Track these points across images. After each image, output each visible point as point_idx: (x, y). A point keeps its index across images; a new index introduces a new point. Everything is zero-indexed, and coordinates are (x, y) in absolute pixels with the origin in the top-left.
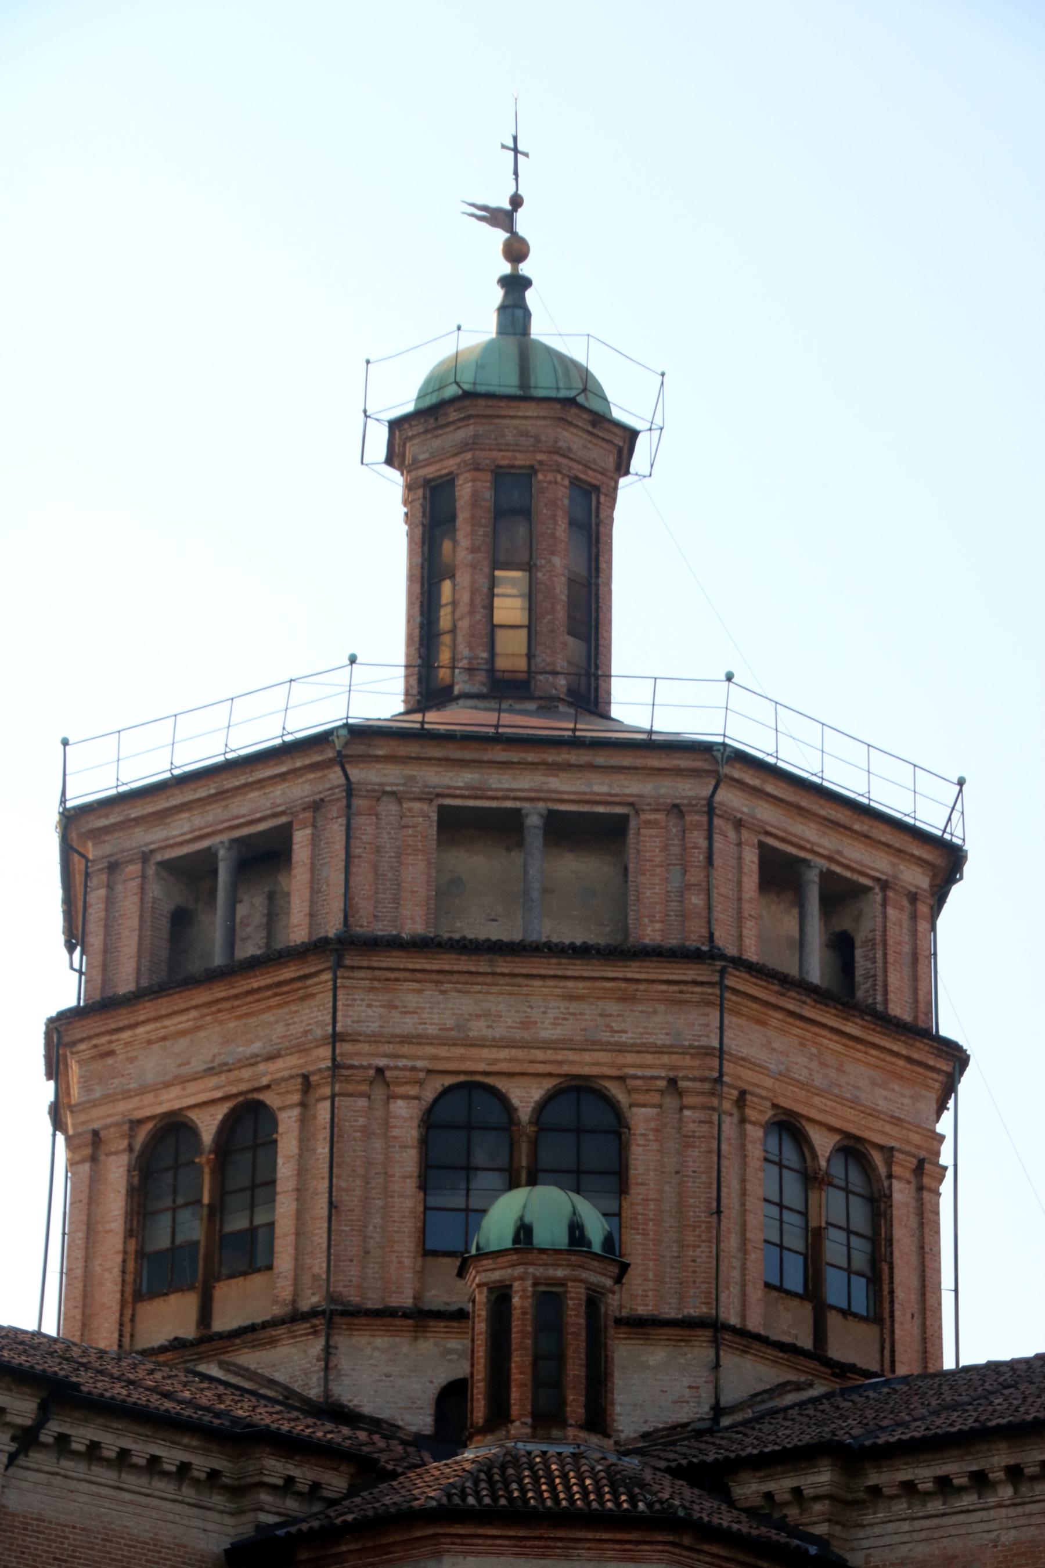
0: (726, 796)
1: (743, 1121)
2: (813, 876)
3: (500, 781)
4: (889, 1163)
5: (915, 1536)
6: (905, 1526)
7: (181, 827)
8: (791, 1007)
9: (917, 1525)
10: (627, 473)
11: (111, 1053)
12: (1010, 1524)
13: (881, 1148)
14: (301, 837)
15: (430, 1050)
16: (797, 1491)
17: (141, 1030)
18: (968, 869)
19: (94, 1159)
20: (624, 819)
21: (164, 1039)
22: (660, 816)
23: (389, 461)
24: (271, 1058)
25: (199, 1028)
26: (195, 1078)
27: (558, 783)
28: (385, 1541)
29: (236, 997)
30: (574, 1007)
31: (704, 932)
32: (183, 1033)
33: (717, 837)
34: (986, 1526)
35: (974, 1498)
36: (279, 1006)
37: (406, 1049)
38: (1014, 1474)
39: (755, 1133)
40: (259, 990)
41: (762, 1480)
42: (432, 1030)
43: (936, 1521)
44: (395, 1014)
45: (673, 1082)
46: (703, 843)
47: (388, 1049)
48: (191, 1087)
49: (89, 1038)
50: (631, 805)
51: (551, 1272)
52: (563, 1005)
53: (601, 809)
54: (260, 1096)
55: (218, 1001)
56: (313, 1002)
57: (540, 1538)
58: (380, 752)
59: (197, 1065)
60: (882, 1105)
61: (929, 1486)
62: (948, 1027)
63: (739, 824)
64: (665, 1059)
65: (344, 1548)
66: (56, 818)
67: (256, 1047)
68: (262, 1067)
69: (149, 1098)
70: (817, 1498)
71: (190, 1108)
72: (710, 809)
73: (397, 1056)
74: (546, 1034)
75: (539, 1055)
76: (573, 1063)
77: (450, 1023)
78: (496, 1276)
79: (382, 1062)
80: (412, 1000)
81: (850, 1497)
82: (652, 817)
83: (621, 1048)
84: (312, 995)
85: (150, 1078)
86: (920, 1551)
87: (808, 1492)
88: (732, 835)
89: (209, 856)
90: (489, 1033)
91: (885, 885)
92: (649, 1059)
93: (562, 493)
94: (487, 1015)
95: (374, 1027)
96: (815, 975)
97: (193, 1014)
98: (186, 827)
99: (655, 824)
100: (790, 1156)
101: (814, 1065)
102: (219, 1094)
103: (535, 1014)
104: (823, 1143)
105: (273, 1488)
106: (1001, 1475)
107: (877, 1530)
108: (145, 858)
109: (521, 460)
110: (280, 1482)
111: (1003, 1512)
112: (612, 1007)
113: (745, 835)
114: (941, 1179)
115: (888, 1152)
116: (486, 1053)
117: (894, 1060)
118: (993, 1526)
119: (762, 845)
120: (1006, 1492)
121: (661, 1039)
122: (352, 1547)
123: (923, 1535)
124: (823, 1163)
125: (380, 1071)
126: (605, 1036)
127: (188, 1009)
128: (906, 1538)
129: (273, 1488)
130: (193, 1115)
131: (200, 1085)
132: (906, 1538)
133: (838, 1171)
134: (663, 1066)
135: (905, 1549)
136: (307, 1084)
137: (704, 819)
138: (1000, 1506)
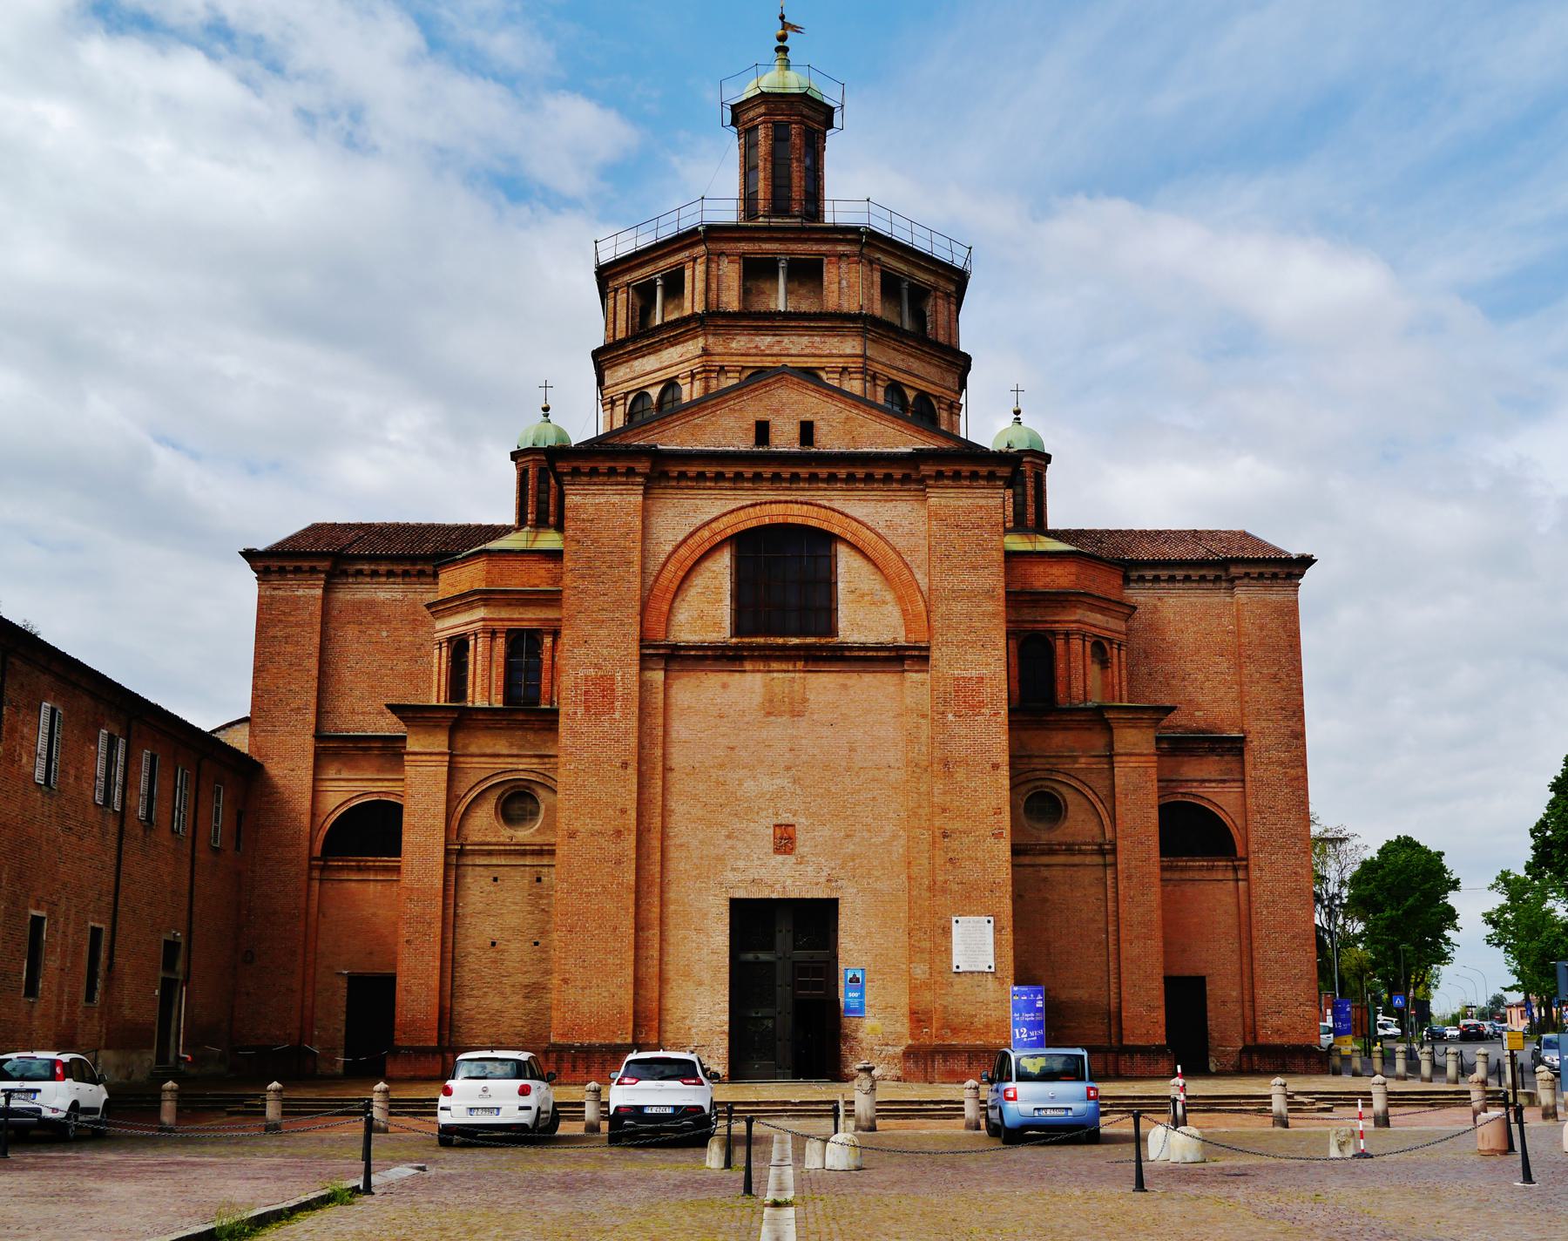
1: (875, 385)
10: (832, 127)
13: (935, 397)
14: (688, 273)
19: (612, 409)
23: (733, 124)
27: (794, 247)
62: (964, 347)
66: (594, 269)
91: (936, 289)
96: (907, 327)
100: (896, 399)
104: (911, 395)
108: (628, 285)
114: (960, 410)
119: (882, 272)
136: (693, 376)
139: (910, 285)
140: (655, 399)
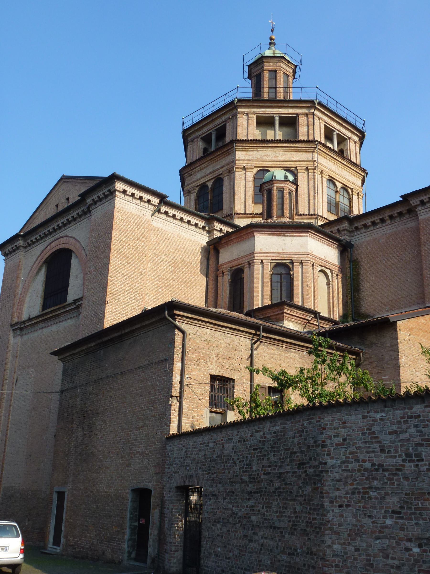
0: (316, 112)
2: (335, 133)
3: (269, 110)
4: (352, 191)
5: (366, 236)
6: (364, 234)
7: (205, 129)
8: (332, 155)
9: (367, 233)
11: (192, 175)
12: (390, 228)
15: (255, 162)
16: (338, 230)
17: (197, 168)
18: (366, 137)
20: (295, 118)
21: (201, 169)
22: (303, 116)
23: (248, 78)
24: (222, 168)
25: (208, 166)
26: (208, 175)
28: (241, 235)
29: (215, 157)
30: (286, 153)
31: (313, 138)
32: (205, 168)
33: (315, 120)
34: (383, 231)
35: (381, 225)
36: (223, 158)
37: (250, 162)
38: (391, 217)
39: (325, 180)
40: (220, 154)
41: (330, 228)
42: (255, 159)
43: (371, 232)
44: (248, 156)
45: (307, 168)
46: (312, 121)
47: (245, 162)
48: (206, 177)
49: (187, 172)
50: (297, 114)
51: (280, 185)
52: (283, 153)
53: (291, 115)
54: (220, 176)
55: (212, 159)
56: (230, 155)
57: (278, 231)
58: (244, 105)
59: (208, 173)
60: (350, 180)
61: (370, 224)
63: (320, 119)
64: (305, 163)
65: (232, 238)
67: (219, 167)
68: (220, 170)
69: (199, 181)
70: (343, 230)
71: (206, 182)
72: (314, 114)
73: (248, 164)
74: (279, 159)
75: (278, 163)
76: (285, 164)
77: (259, 157)
78: (268, 187)
79: (244, 165)
80: (251, 153)
81: (350, 230)
82: (301, 116)
83: (295, 161)
84: (230, 154)
85: (199, 177)
86: (367, 239)
87: (341, 229)
88: (318, 121)
89: (211, 134)
90: (267, 159)
91: (350, 138)
92: (302, 163)
93: (282, 74)
94: (267, 155)
95: (243, 158)
97: (207, 163)
98: (206, 129)
99: (302, 118)
101: (336, 169)
102: (212, 177)
103: (277, 155)
104: (339, 186)
105: (217, 230)
106: (388, 218)
107: (357, 237)
109: (274, 69)
110: (219, 229)
111: (388, 226)
112: (294, 153)
113: (321, 121)
115: (352, 189)
116: (267, 163)
117: (353, 171)
118: (385, 230)
120: (389, 222)
121: (304, 159)
122: (234, 238)
123: (368, 235)
124: (339, 189)
125: (244, 167)
126: (293, 159)
127: (206, 162)
128: (364, 237)
129: (217, 230)
130: (207, 183)
131: (208, 176)
132: (364, 237)
133: (342, 191)
134: (305, 164)
135: (363, 240)
137: (312, 116)
138: (387, 225)
139: (338, 134)
140: (210, 187)
